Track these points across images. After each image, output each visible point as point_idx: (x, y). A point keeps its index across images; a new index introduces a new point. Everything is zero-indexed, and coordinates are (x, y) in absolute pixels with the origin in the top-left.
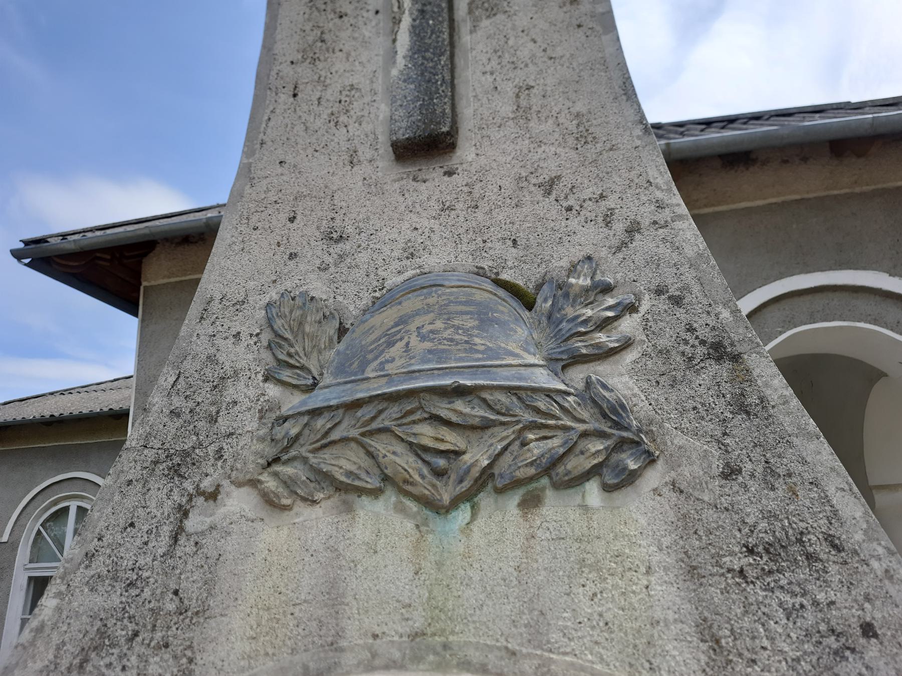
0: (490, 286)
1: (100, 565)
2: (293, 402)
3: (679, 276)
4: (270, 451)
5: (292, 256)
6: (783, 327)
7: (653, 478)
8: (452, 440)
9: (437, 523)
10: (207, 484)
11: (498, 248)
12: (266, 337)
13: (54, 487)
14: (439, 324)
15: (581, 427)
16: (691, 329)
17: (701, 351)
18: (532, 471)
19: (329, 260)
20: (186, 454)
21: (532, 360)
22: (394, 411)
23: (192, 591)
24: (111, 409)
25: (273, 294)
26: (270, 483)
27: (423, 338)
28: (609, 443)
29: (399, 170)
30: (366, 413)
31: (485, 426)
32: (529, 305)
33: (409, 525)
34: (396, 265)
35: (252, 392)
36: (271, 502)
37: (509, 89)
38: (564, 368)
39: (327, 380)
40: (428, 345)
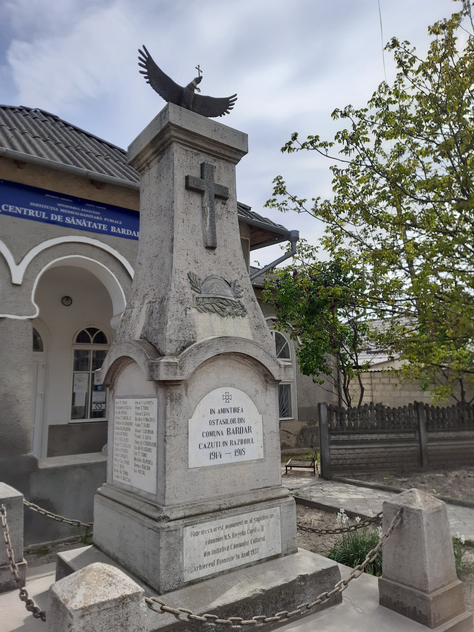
1: (175, 317)
7: (247, 316)
8: (224, 307)
11: (224, 274)
25: (188, 271)
26: (199, 308)
29: (205, 250)
32: (230, 286)
39: (203, 292)
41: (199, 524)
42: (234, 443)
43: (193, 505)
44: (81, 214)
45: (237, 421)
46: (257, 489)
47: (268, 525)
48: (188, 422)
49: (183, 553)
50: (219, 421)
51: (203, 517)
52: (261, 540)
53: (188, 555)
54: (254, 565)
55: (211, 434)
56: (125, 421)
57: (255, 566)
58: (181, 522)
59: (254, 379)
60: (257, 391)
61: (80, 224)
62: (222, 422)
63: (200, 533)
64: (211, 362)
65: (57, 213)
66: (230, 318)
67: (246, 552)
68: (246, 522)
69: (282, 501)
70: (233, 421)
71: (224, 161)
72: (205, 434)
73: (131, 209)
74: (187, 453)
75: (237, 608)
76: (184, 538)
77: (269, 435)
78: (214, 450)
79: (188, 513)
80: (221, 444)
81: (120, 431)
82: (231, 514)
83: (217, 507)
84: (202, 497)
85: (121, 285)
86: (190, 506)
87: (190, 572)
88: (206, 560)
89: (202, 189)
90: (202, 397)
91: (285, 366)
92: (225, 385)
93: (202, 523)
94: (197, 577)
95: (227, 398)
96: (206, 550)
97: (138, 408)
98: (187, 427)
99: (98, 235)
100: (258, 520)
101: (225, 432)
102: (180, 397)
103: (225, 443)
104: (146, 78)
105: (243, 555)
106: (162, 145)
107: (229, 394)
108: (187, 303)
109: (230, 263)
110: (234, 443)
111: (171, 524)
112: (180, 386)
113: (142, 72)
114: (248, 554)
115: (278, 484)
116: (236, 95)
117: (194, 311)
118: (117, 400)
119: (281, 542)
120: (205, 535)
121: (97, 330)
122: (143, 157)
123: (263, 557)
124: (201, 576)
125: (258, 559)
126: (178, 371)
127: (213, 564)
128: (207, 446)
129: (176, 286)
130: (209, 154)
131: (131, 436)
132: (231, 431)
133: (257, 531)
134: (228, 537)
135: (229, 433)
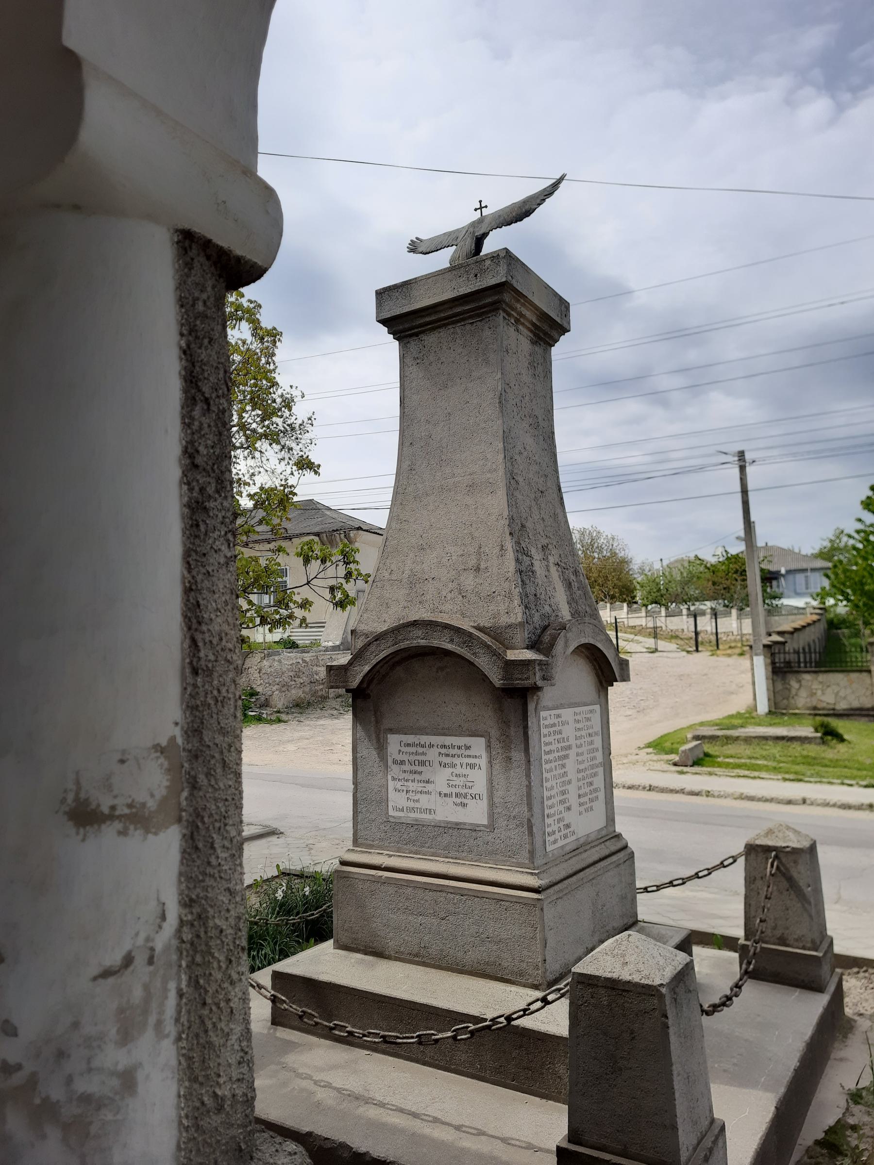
56: (559, 746)
81: (553, 765)
97: (578, 721)
106: (546, 334)
118: (543, 714)
122: (523, 305)
131: (571, 765)
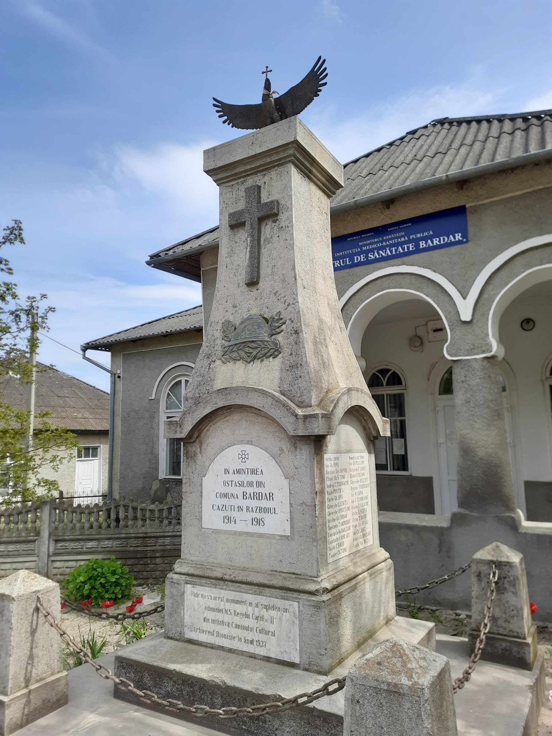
0: (261, 319)
1: (198, 374)
2: (227, 344)
3: (294, 316)
4: (223, 354)
5: (227, 311)
6: (524, 268)
7: (280, 356)
9: (248, 365)
10: (213, 360)
12: (222, 330)
13: (173, 370)
14: (251, 328)
15: (271, 347)
16: (293, 328)
17: (294, 332)
18: (262, 356)
19: (234, 312)
20: (210, 354)
21: (265, 335)
22: (243, 345)
23: (212, 377)
24: (195, 327)
26: (223, 359)
27: (248, 331)
28: (274, 350)
30: (238, 346)
31: (256, 348)
33: (244, 365)
34: (246, 313)
35: (220, 342)
36: (224, 363)
37: (271, 266)
38: (271, 336)
40: (249, 332)
41: (198, 585)
42: (250, 509)
43: (202, 565)
44: (384, 244)
45: (255, 484)
46: (280, 572)
47: (281, 619)
48: (202, 480)
49: (184, 609)
50: (233, 483)
51: (204, 581)
52: (270, 633)
53: (189, 613)
54: (260, 659)
55: (225, 495)
57: (259, 661)
58: (183, 577)
59: (277, 434)
60: (282, 450)
61: (384, 254)
62: (238, 484)
63: (200, 596)
64: (225, 417)
65: (359, 254)
66: (257, 363)
67: (250, 639)
68: (251, 604)
69: (303, 597)
70: (250, 484)
71: (276, 168)
72: (218, 495)
73: (444, 208)
74: (201, 512)
75: (192, 683)
76: (186, 595)
77: (299, 508)
78: (228, 513)
79: (191, 571)
80: (236, 509)
82: (232, 588)
83: (219, 575)
84: (214, 560)
85: (441, 310)
86: (199, 566)
87: (190, 629)
88: (206, 626)
89: (243, 220)
90: (216, 455)
91: (304, 416)
92: (241, 442)
93: (202, 586)
94: (197, 639)
95: (244, 457)
96: (205, 615)
98: (201, 485)
99: (406, 259)
100: (267, 608)
101: (240, 496)
102: (195, 455)
103: (240, 508)
104: (229, 124)
105: (246, 641)
107: (246, 453)
108: (213, 356)
109: (275, 294)
110: (250, 509)
111: (176, 576)
112: (195, 444)
113: (224, 122)
114: (252, 642)
115: (312, 575)
116: (320, 58)
117: (218, 362)
119: (298, 647)
120: (205, 599)
121: (390, 370)
123: (272, 656)
124: (200, 640)
125: (265, 655)
126: (178, 429)
127: (211, 633)
128: (221, 508)
129: (208, 341)
130: (256, 173)
132: (248, 496)
133: (265, 620)
134: (229, 612)
135: (245, 497)
